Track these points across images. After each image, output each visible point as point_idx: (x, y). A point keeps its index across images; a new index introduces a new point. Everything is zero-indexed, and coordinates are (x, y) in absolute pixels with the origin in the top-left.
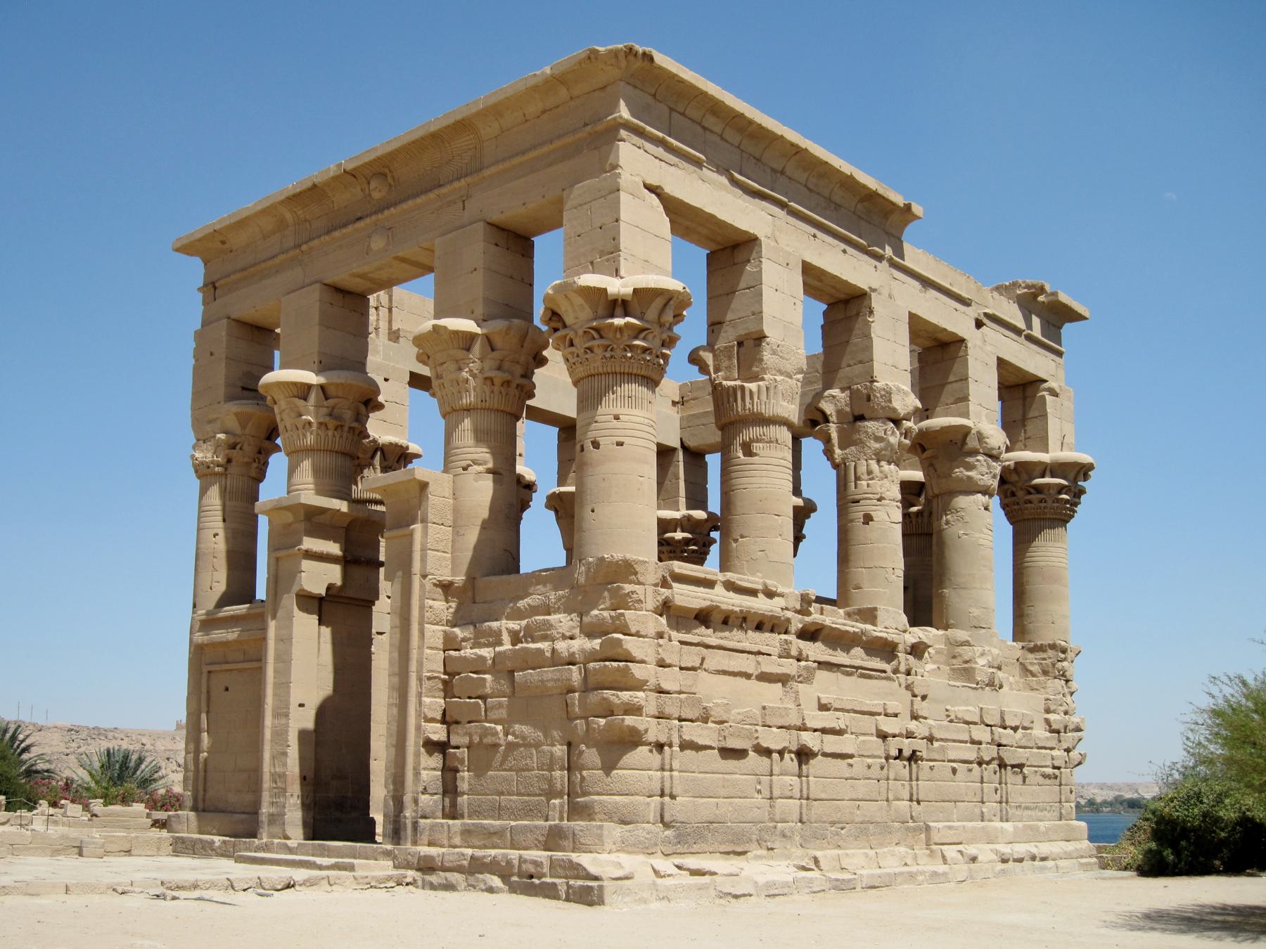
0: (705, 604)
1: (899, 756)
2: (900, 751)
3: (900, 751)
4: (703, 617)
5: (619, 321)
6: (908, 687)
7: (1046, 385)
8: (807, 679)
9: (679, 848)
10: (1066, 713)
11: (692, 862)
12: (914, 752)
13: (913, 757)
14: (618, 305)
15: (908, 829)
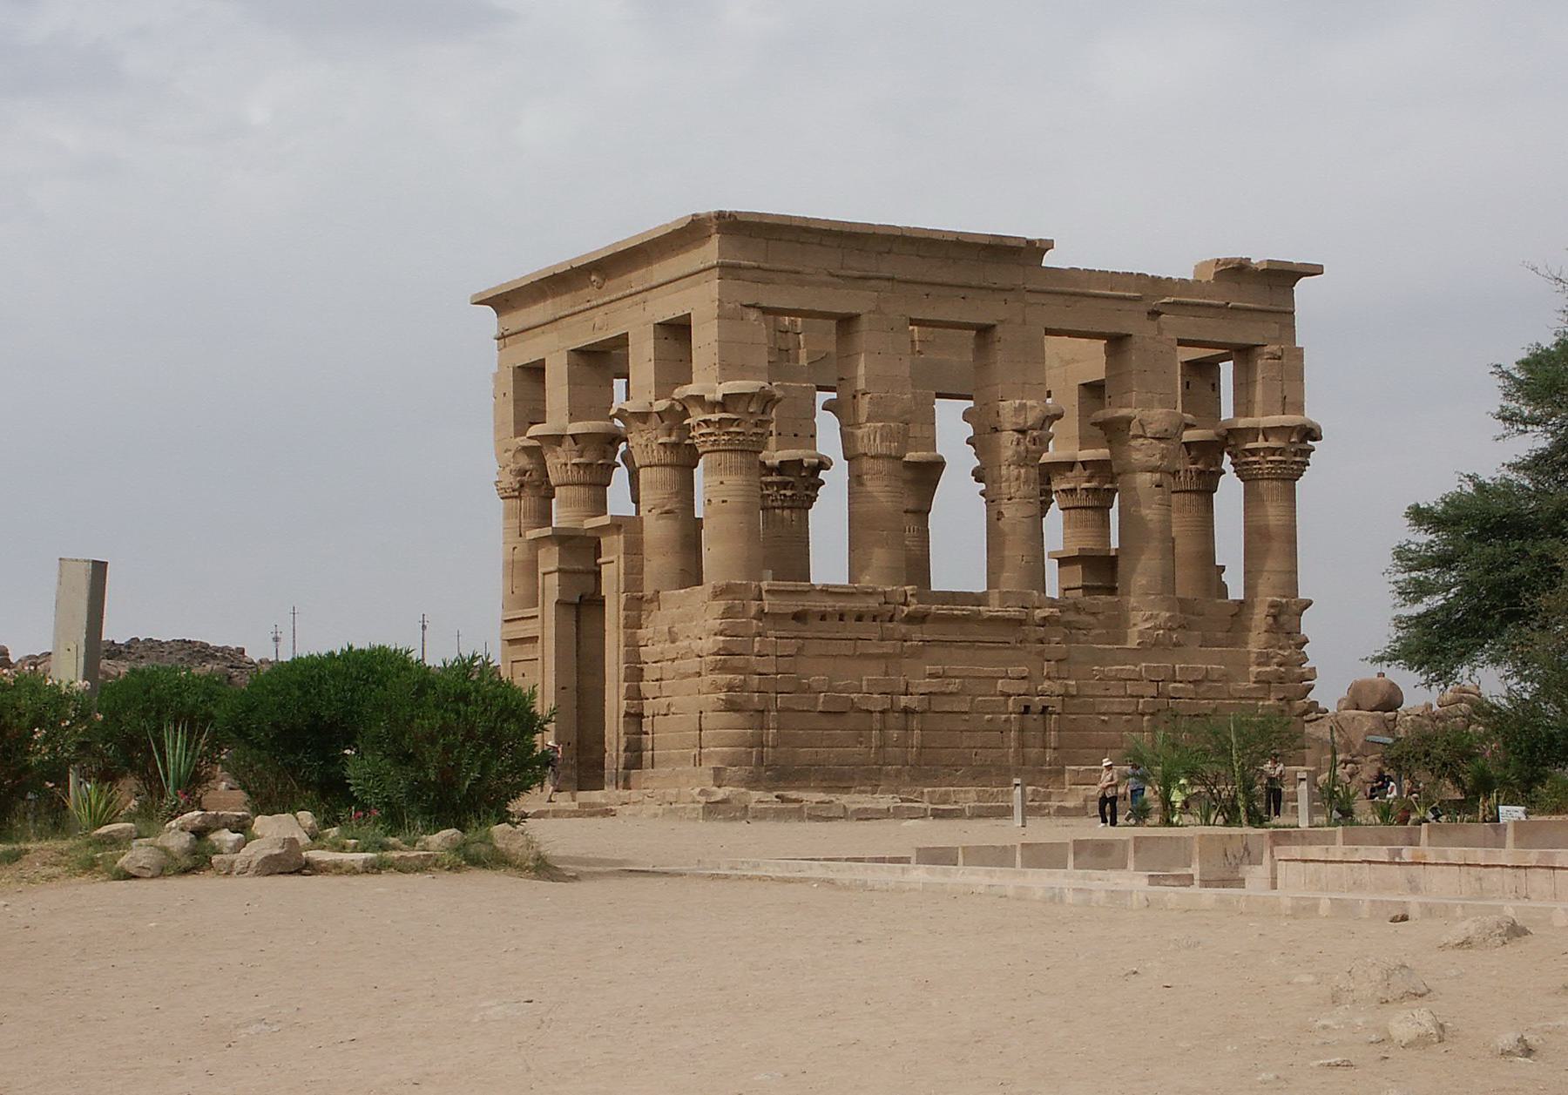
0: (795, 609)
1: (1027, 709)
2: (1027, 708)
3: (1027, 708)
4: (799, 617)
5: (715, 417)
6: (1040, 653)
7: (1266, 349)
8: (915, 654)
9: (782, 784)
10: (1280, 665)
11: (793, 794)
12: (1045, 708)
13: (1044, 710)
14: (714, 406)
15: (1042, 772)
